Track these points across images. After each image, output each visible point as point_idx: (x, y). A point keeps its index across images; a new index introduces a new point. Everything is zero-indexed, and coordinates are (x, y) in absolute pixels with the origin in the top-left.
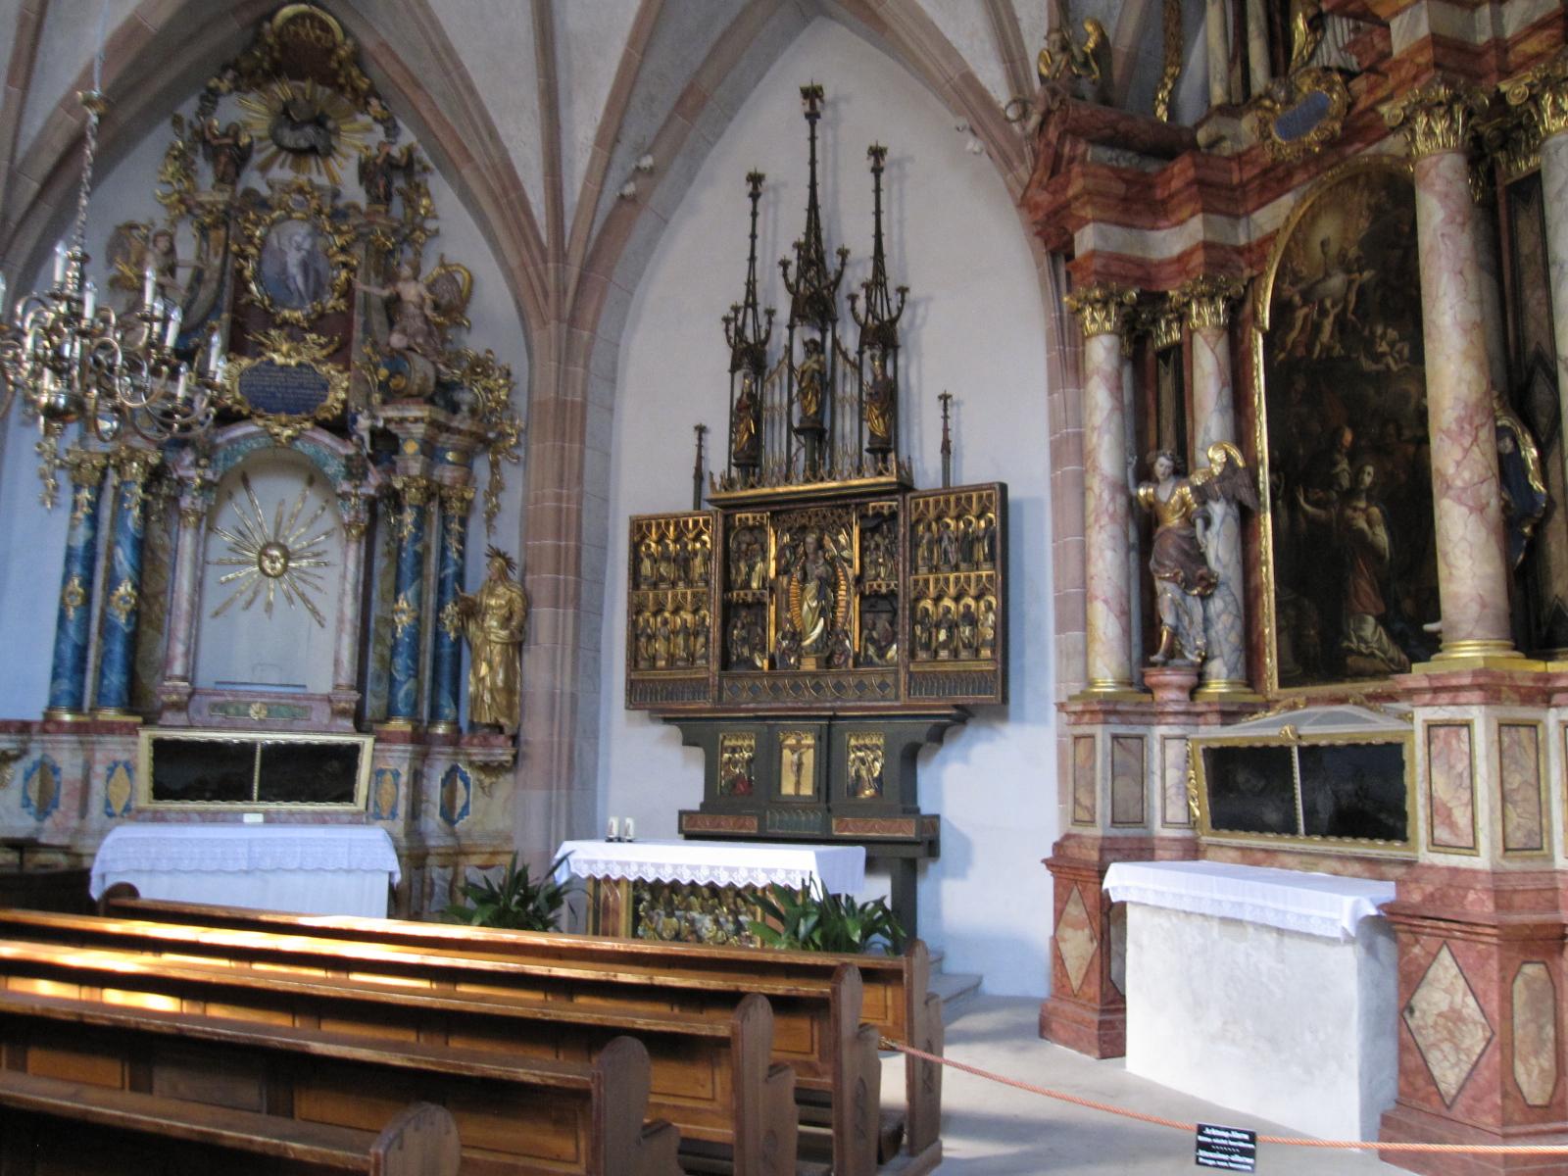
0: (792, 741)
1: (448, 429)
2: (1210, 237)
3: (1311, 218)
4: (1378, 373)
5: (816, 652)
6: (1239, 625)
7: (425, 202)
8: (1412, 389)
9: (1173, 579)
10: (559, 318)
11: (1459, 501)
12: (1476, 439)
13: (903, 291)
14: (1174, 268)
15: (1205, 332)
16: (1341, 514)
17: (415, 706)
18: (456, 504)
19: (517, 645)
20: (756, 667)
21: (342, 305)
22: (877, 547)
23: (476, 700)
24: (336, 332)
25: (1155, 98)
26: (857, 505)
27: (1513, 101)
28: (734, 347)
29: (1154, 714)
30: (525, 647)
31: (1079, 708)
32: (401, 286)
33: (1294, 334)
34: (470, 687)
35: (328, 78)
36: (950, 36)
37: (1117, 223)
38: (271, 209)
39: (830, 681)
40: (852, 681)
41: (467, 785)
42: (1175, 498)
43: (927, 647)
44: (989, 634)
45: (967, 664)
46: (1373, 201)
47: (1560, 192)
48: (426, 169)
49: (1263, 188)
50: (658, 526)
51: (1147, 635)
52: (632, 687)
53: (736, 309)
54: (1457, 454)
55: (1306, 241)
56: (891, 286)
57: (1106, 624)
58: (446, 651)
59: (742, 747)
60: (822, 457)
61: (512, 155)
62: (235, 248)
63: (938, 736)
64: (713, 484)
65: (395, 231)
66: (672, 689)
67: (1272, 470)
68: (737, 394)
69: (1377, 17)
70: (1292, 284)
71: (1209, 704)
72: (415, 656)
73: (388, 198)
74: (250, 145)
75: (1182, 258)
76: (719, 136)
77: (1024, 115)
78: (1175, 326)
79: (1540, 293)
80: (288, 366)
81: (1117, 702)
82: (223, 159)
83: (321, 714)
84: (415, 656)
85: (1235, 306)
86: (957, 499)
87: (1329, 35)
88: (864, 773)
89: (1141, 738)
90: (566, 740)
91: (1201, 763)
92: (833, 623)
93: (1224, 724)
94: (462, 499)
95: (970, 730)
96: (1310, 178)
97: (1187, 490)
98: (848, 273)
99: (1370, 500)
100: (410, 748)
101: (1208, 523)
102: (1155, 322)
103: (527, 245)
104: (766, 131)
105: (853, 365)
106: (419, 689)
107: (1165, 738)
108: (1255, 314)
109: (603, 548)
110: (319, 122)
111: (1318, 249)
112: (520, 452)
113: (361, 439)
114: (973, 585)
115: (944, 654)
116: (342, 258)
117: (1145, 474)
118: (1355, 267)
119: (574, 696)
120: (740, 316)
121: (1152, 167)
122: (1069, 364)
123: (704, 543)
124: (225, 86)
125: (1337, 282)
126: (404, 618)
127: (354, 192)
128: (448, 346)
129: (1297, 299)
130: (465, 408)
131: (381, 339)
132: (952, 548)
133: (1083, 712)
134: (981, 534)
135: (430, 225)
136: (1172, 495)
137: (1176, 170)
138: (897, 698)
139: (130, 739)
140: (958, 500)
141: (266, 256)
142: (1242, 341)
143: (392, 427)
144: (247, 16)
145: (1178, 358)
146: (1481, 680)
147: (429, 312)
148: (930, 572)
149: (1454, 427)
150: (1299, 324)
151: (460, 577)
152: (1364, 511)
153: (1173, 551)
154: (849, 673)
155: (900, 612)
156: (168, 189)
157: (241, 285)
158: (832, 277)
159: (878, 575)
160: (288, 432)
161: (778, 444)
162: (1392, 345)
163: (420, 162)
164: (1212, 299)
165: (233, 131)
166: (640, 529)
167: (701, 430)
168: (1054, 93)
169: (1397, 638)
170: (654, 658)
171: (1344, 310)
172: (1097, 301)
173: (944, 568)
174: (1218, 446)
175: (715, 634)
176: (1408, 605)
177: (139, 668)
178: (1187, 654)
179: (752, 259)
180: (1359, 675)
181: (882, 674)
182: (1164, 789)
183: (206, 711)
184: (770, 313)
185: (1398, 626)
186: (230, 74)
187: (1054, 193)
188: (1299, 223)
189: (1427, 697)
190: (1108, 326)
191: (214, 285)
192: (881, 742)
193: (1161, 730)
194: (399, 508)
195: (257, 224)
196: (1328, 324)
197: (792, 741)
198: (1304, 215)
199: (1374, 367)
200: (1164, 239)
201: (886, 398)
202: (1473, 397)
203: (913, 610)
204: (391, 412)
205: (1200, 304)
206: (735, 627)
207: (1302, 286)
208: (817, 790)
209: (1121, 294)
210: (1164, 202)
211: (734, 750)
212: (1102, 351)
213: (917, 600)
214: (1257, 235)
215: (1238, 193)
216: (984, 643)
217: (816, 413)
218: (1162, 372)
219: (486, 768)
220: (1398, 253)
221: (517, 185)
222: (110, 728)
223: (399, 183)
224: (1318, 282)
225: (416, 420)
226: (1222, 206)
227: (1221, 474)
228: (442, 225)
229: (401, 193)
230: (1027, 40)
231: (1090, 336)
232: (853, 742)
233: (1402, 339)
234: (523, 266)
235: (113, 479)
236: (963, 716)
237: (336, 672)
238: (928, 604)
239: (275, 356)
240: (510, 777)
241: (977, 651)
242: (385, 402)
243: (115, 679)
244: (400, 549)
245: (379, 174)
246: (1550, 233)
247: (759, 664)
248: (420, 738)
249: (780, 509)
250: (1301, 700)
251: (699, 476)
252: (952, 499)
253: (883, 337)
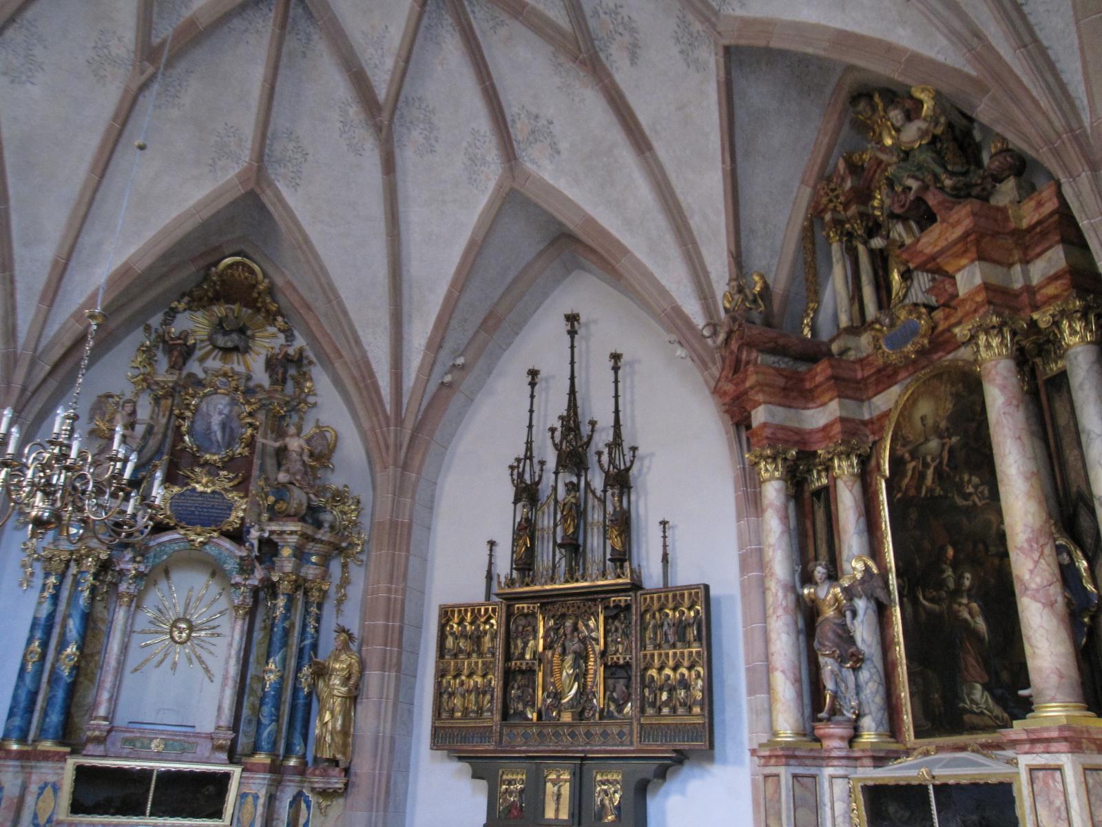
0: (553, 776)
1: (314, 540)
2: (844, 414)
3: (913, 401)
4: (968, 507)
5: (572, 708)
6: (882, 690)
7: (308, 384)
8: (993, 517)
9: (831, 656)
10: (395, 464)
11: (1034, 598)
12: (1042, 554)
13: (634, 449)
14: (820, 435)
15: (845, 478)
16: (950, 608)
17: (275, 744)
18: (316, 594)
19: (353, 698)
20: (528, 719)
21: (246, 452)
22: (616, 630)
23: (320, 740)
24: (240, 472)
25: (802, 323)
26: (603, 599)
27: (1043, 325)
28: (517, 486)
29: (823, 758)
30: (358, 700)
31: (767, 753)
32: (287, 440)
33: (906, 481)
34: (316, 730)
35: (251, 303)
36: (664, 282)
37: (780, 405)
38: (204, 386)
39: (582, 730)
40: (598, 730)
41: (308, 807)
42: (830, 596)
43: (653, 704)
44: (699, 695)
45: (682, 718)
46: (954, 390)
47: (1081, 385)
48: (311, 363)
49: (878, 382)
50: (460, 612)
51: (816, 699)
52: (436, 731)
53: (518, 460)
54: (1030, 565)
55: (910, 417)
56: (626, 445)
57: (785, 689)
58: (301, 701)
59: (516, 779)
60: (577, 564)
61: (370, 355)
62: (177, 412)
63: (662, 774)
64: (499, 583)
65: (287, 403)
66: (465, 735)
67: (899, 575)
68: (518, 519)
69: (947, 272)
70: (903, 446)
71: (863, 751)
72: (277, 707)
73: (284, 381)
74: (195, 344)
75: (825, 428)
76: (511, 343)
77: (715, 334)
78: (823, 474)
79: (1076, 452)
80: (206, 493)
81: (795, 749)
82: (176, 353)
83: (204, 748)
84: (277, 707)
85: (864, 461)
86: (674, 595)
87: (915, 283)
88: (607, 802)
89: (814, 777)
90: (385, 772)
91: (861, 797)
92: (585, 685)
93: (875, 767)
94: (320, 590)
95: (686, 770)
96: (910, 375)
97: (838, 590)
98: (596, 437)
99: (970, 597)
100: (268, 776)
101: (854, 614)
102: (809, 471)
103: (377, 415)
104: (542, 342)
105: (599, 499)
106: (278, 731)
107: (832, 777)
108: (879, 467)
109: (419, 627)
110: (242, 331)
112: (363, 557)
113: (252, 545)
114: (686, 658)
115: (665, 710)
116: (249, 420)
117: (807, 579)
118: (946, 434)
119: (392, 739)
120: (521, 465)
121: (802, 368)
122: (751, 501)
123: (492, 625)
124: (182, 306)
125: (934, 444)
126: (272, 677)
127: (261, 377)
128: (318, 482)
129: (907, 456)
130: (326, 525)
131: (272, 476)
132: (671, 632)
133: (770, 757)
134: (691, 621)
135: (311, 399)
136: (828, 594)
137: (819, 369)
138: (632, 744)
139: (60, 765)
140: (674, 596)
141: (198, 417)
142: (871, 485)
143: (274, 537)
144: (202, 263)
145: (826, 496)
146: (1067, 734)
147: (306, 458)
148: (655, 648)
149: (1025, 545)
150: (909, 473)
151: (315, 646)
152: (967, 605)
153: (830, 635)
154: (596, 724)
155: (633, 678)
156: (136, 372)
157: (179, 436)
158: (585, 439)
159: (617, 651)
160: (201, 539)
161: (546, 554)
162: (976, 487)
163: (307, 358)
164: (848, 456)
165: (184, 335)
166: (446, 614)
167: (492, 544)
168: (734, 319)
169: (999, 700)
170: (453, 711)
172: (769, 457)
173: (665, 646)
174: (859, 558)
175: (498, 693)
176: (1005, 676)
177: (73, 710)
178: (845, 712)
179: (530, 426)
180: (973, 729)
181: (621, 725)
182: (834, 817)
183: (119, 744)
184: (542, 463)
185: (999, 692)
186: (186, 299)
187: (737, 385)
188: (905, 405)
189: (1027, 747)
190: (777, 474)
191: (160, 436)
192: (619, 778)
193: (828, 771)
194: (274, 596)
195: (193, 397)
196: (930, 472)
197: (553, 776)
198: (908, 399)
199: (965, 503)
200: (813, 416)
201: (623, 523)
202: (1038, 524)
203: (643, 676)
204: (274, 527)
205: (840, 459)
206: (513, 688)
207: (909, 447)
208: (572, 815)
209: (785, 452)
210: (811, 391)
211: (510, 783)
212: (773, 491)
213: (646, 669)
214: (876, 413)
215: (861, 386)
216: (695, 703)
217: (573, 533)
218: (816, 506)
219: (324, 793)
220: (974, 425)
221: (372, 375)
222: (46, 756)
223: (292, 371)
224: (922, 444)
225: (292, 533)
226: (850, 393)
227: (862, 578)
228: (319, 400)
229: (293, 378)
230: (715, 285)
231: (765, 481)
232: (599, 778)
233: (982, 484)
234: (373, 429)
235: (73, 569)
236: (681, 758)
237: (219, 716)
238: (653, 672)
239: (197, 486)
240: (341, 801)
241: (690, 709)
242: (270, 520)
243: (55, 718)
244: (273, 625)
245: (280, 365)
246: (1078, 412)
247: (530, 716)
248: (276, 769)
249: (546, 601)
250: (932, 748)
251: (489, 577)
252: (670, 595)
253: (620, 481)
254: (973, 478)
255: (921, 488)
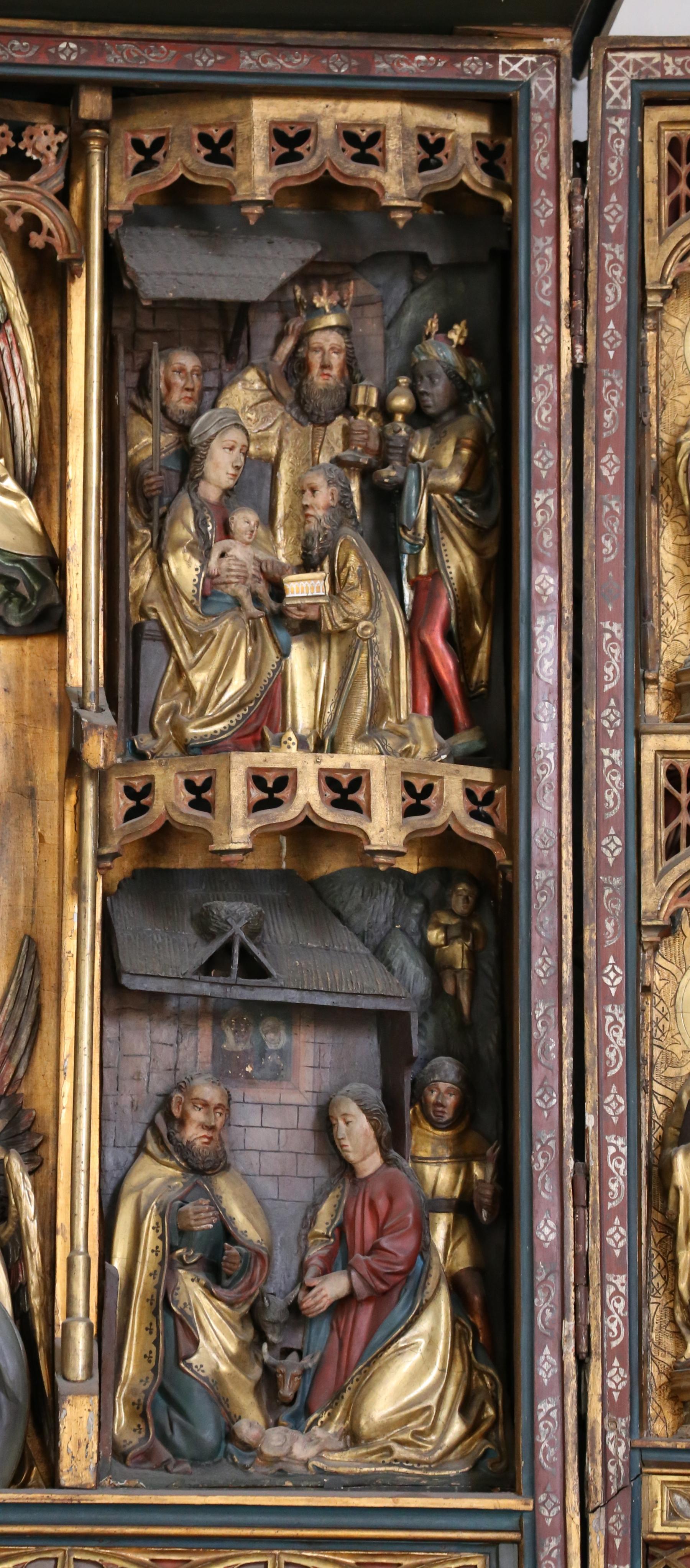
26: (127, 95)
155: (544, 1023)
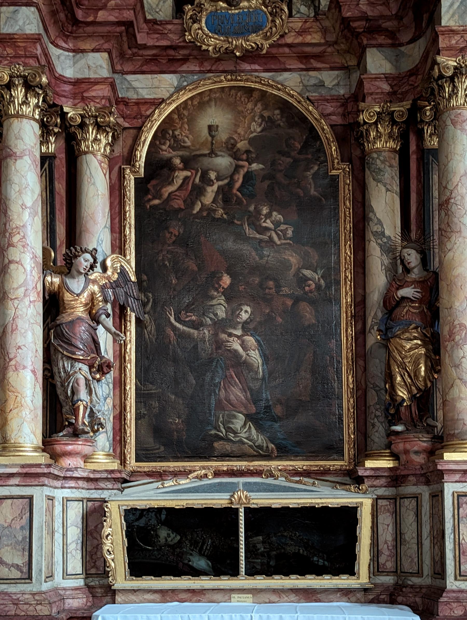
4: (261, 241)
46: (266, 114)
49: (154, 59)
111: (205, 131)
118: (245, 157)
162: (277, 224)
171: (230, 185)
198: (192, 98)
224: (205, 155)
254: (275, 213)
255: (193, 204)
